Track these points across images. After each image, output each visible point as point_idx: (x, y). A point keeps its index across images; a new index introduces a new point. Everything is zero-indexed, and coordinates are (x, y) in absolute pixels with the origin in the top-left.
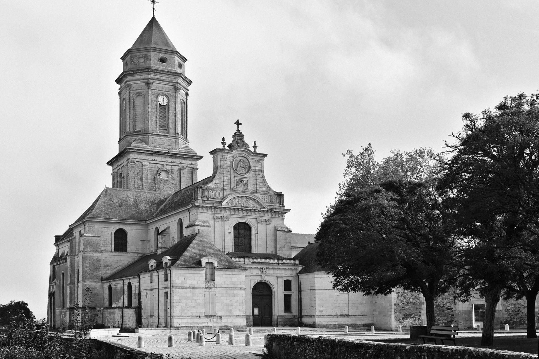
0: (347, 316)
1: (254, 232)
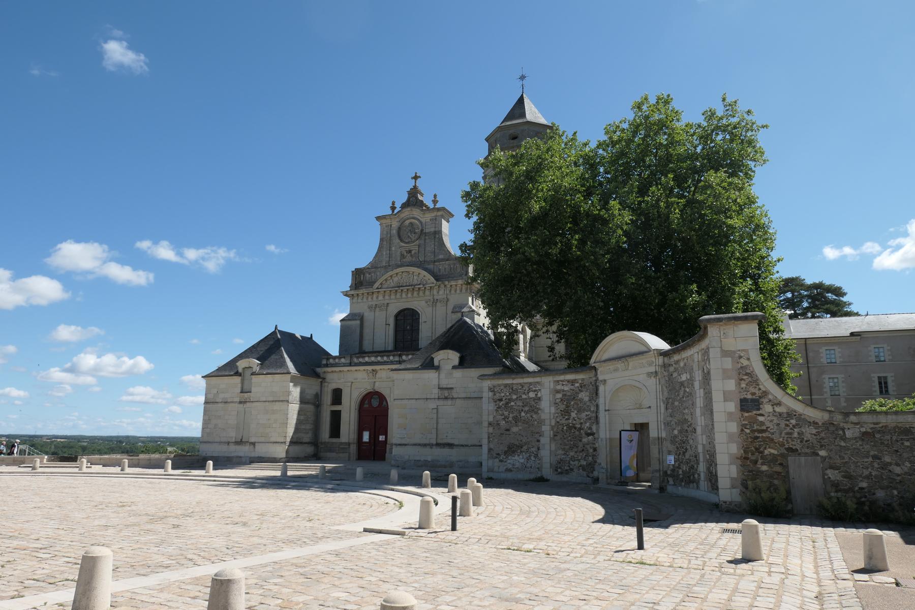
0: (450, 445)
1: (422, 319)
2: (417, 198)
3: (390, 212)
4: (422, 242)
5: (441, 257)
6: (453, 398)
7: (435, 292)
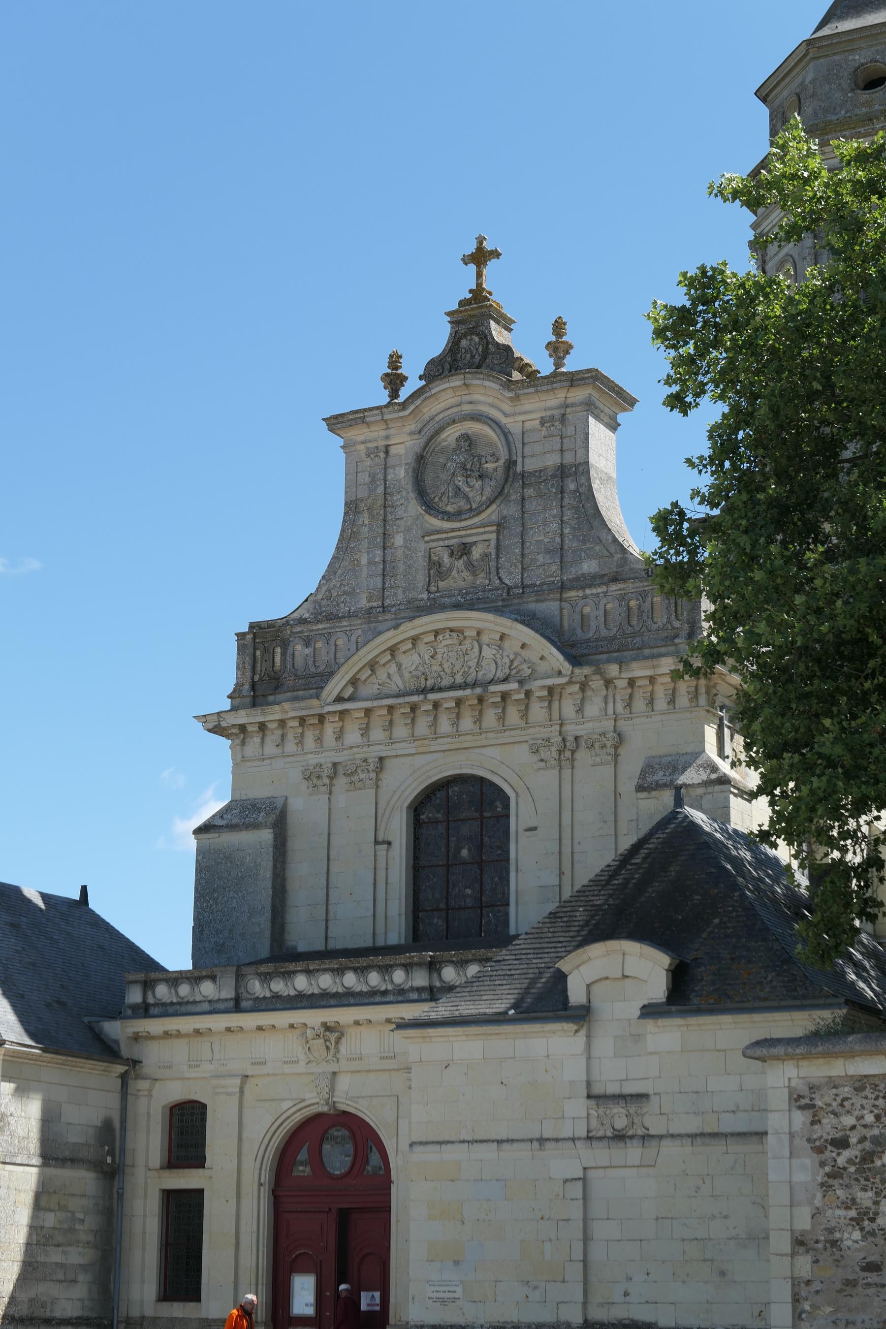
2: (486, 338)
3: (383, 397)
4: (512, 510)
5: (589, 567)
6: (646, 1138)
7: (568, 708)
